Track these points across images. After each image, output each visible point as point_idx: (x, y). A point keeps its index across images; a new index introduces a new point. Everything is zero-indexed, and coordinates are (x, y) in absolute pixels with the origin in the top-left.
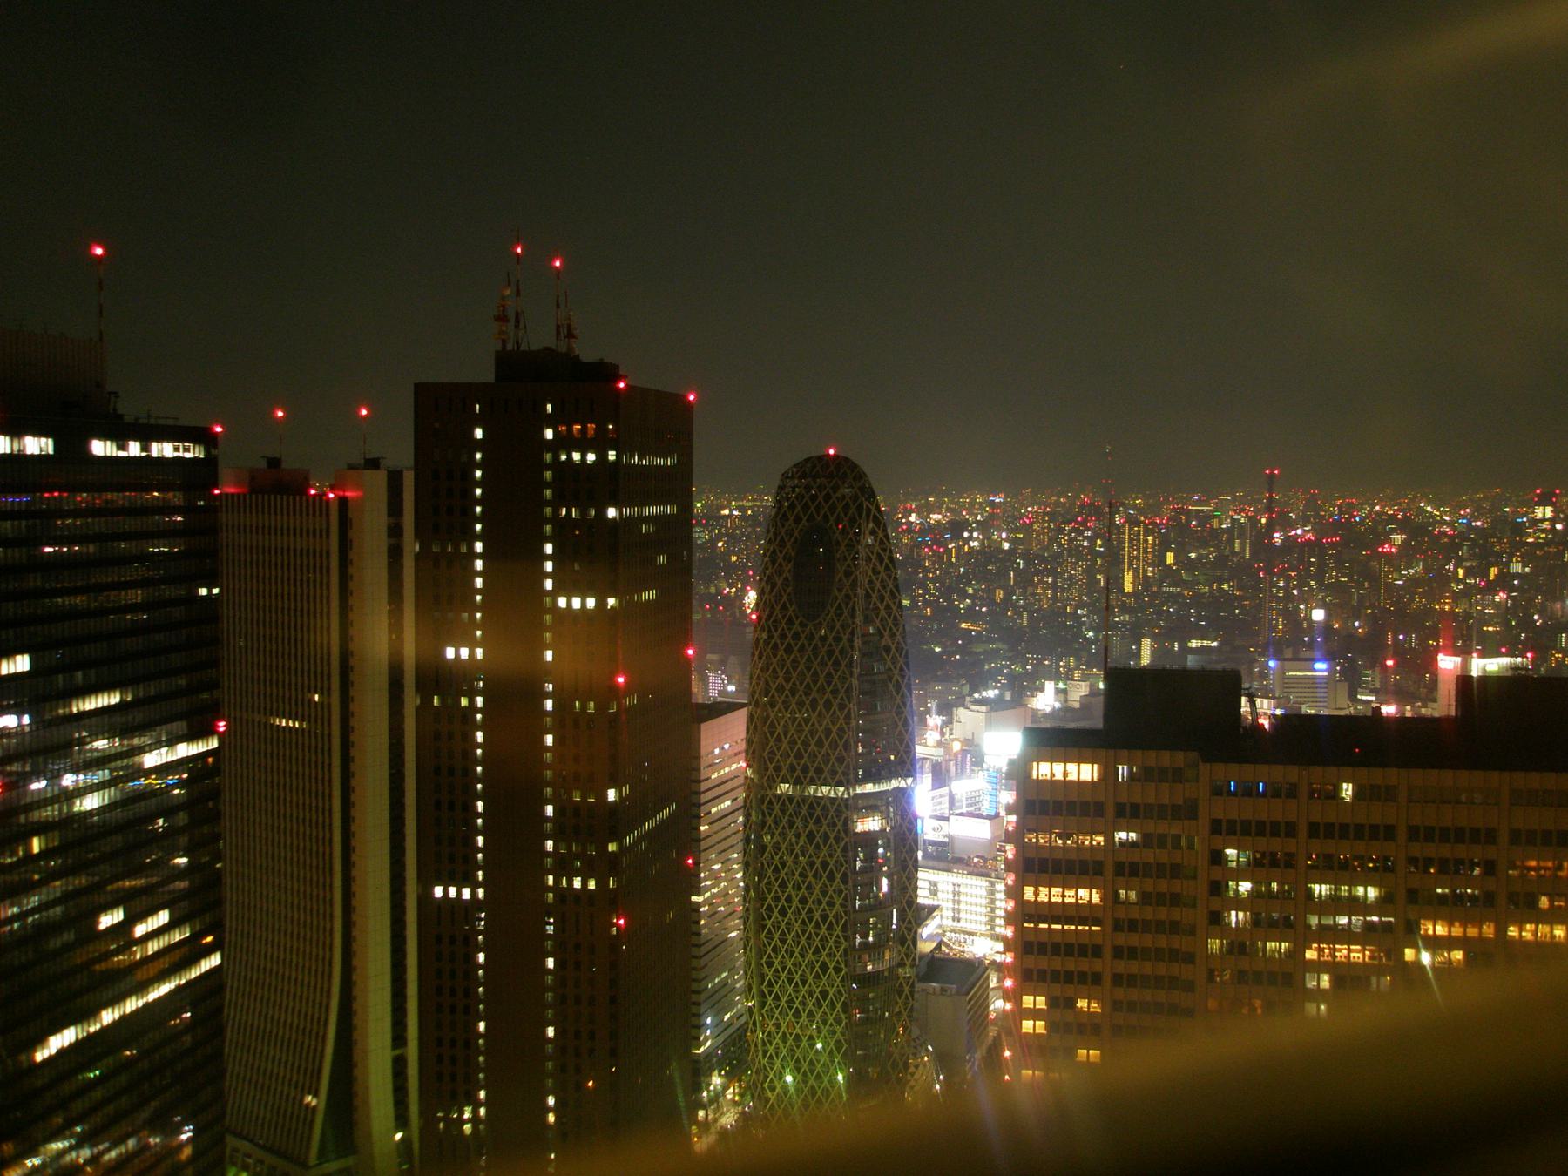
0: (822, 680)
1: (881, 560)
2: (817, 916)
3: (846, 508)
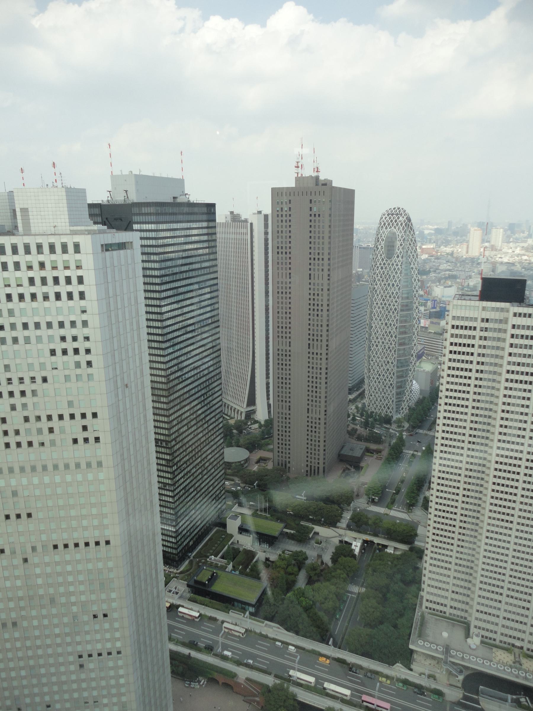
0: (392, 277)
1: (412, 240)
2: (387, 347)
3: (402, 224)
